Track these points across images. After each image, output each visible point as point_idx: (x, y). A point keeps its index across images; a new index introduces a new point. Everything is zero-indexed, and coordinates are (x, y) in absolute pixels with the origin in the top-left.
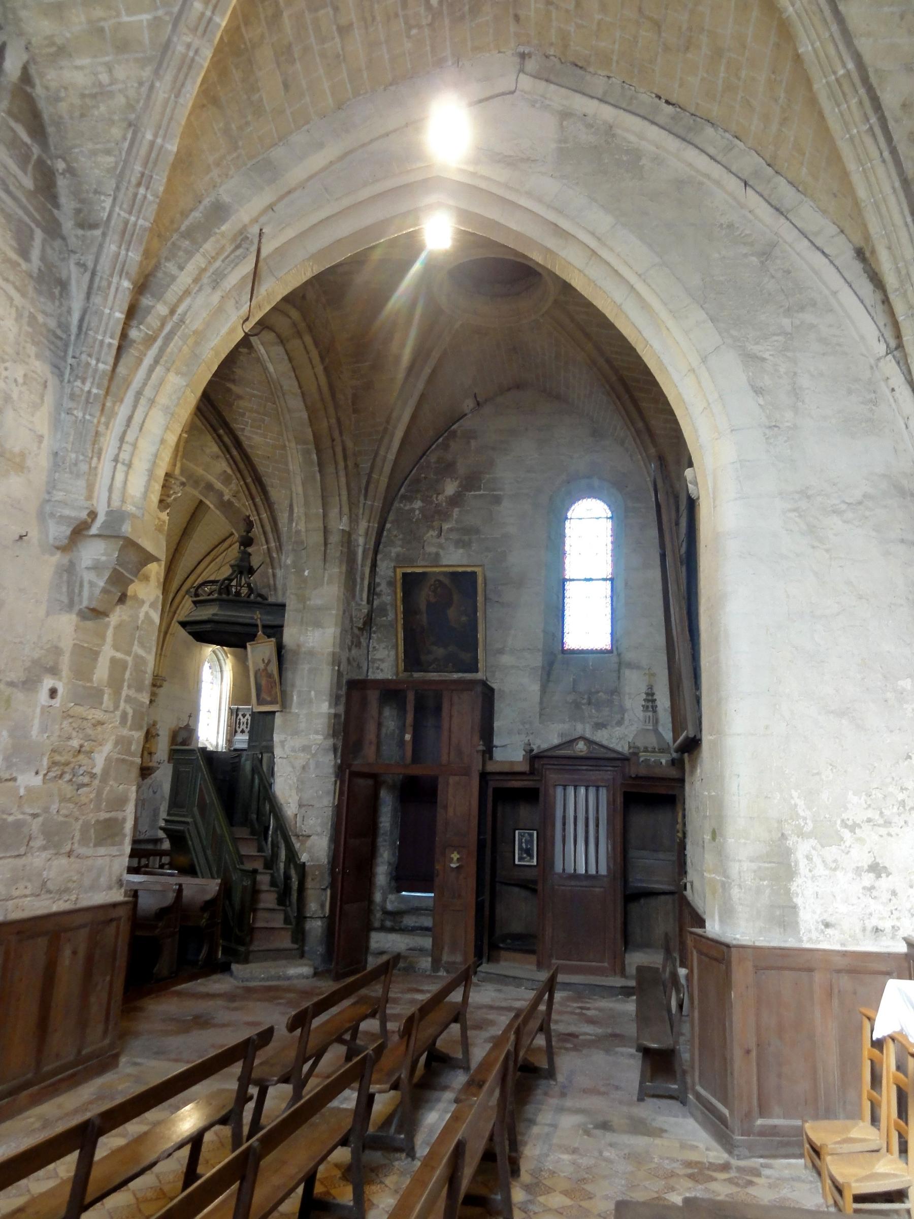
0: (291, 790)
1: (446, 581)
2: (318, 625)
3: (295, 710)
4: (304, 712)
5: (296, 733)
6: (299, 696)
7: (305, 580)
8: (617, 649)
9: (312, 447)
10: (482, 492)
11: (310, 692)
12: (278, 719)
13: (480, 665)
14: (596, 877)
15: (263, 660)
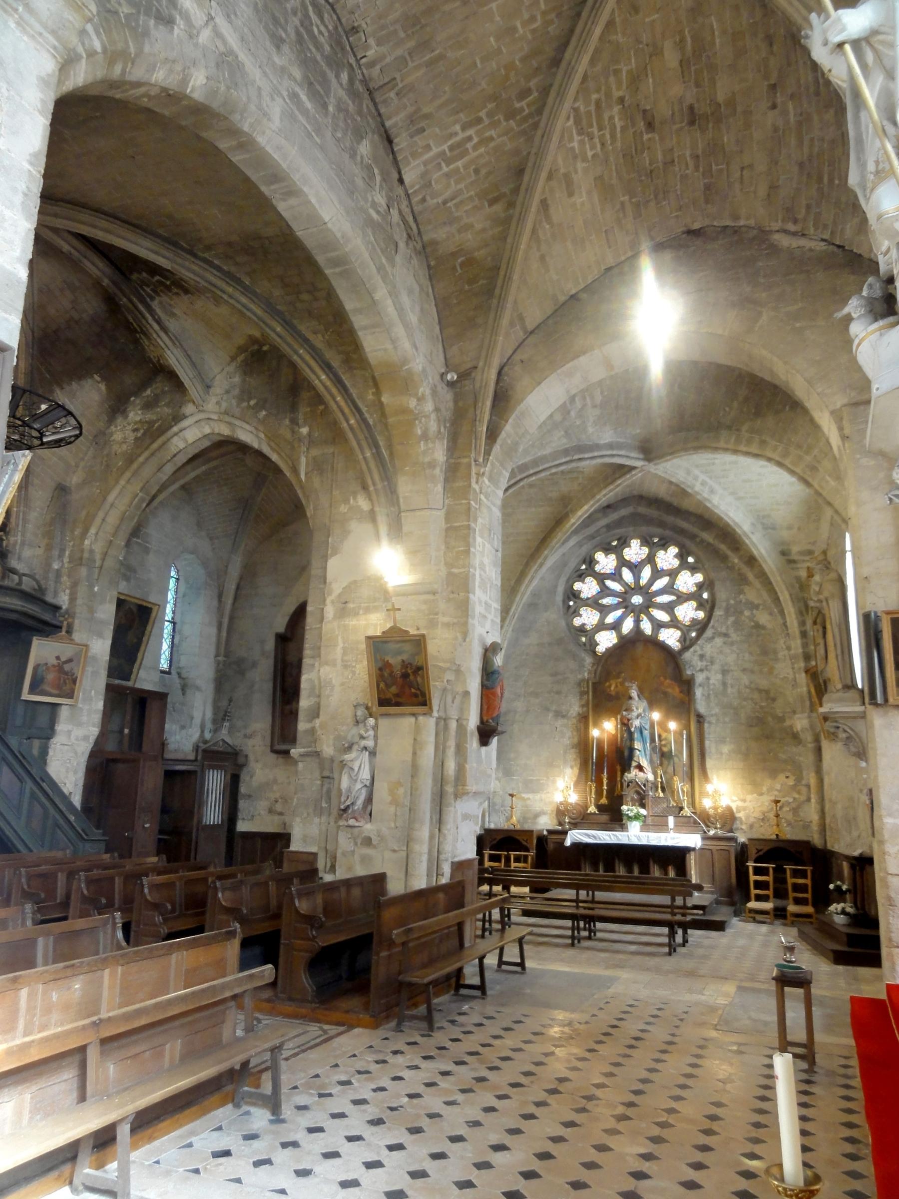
0: (67, 772)
1: (135, 609)
2: (100, 635)
3: (80, 705)
4: (86, 707)
5: (79, 724)
6: (83, 694)
7: (94, 595)
8: (179, 674)
9: (148, 498)
10: (139, 541)
11: (91, 692)
12: (64, 712)
13: (133, 677)
14: (218, 824)
15: (58, 658)
